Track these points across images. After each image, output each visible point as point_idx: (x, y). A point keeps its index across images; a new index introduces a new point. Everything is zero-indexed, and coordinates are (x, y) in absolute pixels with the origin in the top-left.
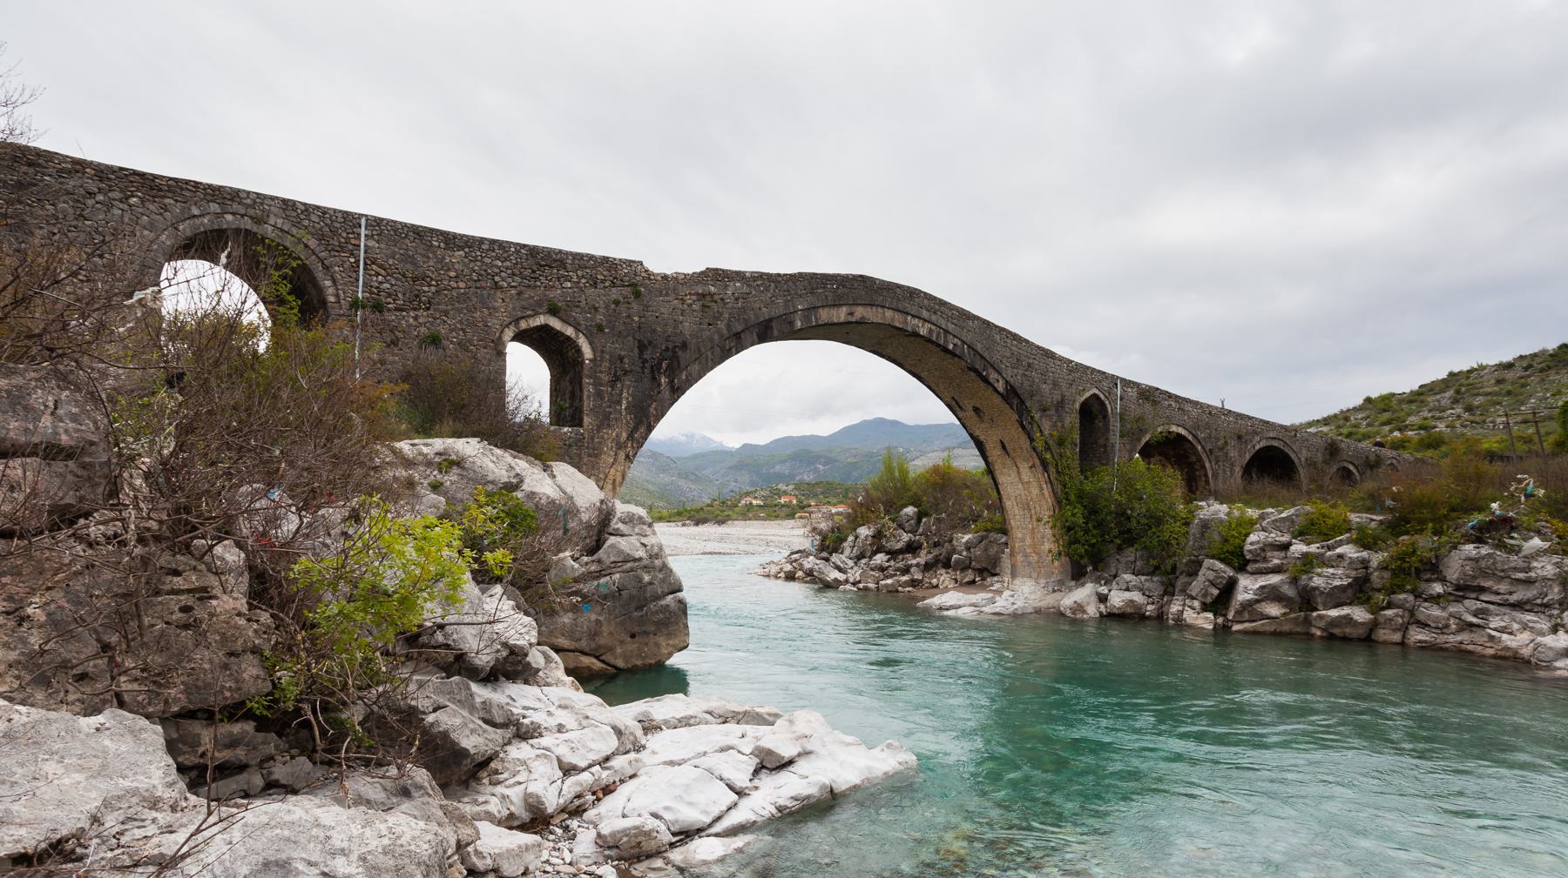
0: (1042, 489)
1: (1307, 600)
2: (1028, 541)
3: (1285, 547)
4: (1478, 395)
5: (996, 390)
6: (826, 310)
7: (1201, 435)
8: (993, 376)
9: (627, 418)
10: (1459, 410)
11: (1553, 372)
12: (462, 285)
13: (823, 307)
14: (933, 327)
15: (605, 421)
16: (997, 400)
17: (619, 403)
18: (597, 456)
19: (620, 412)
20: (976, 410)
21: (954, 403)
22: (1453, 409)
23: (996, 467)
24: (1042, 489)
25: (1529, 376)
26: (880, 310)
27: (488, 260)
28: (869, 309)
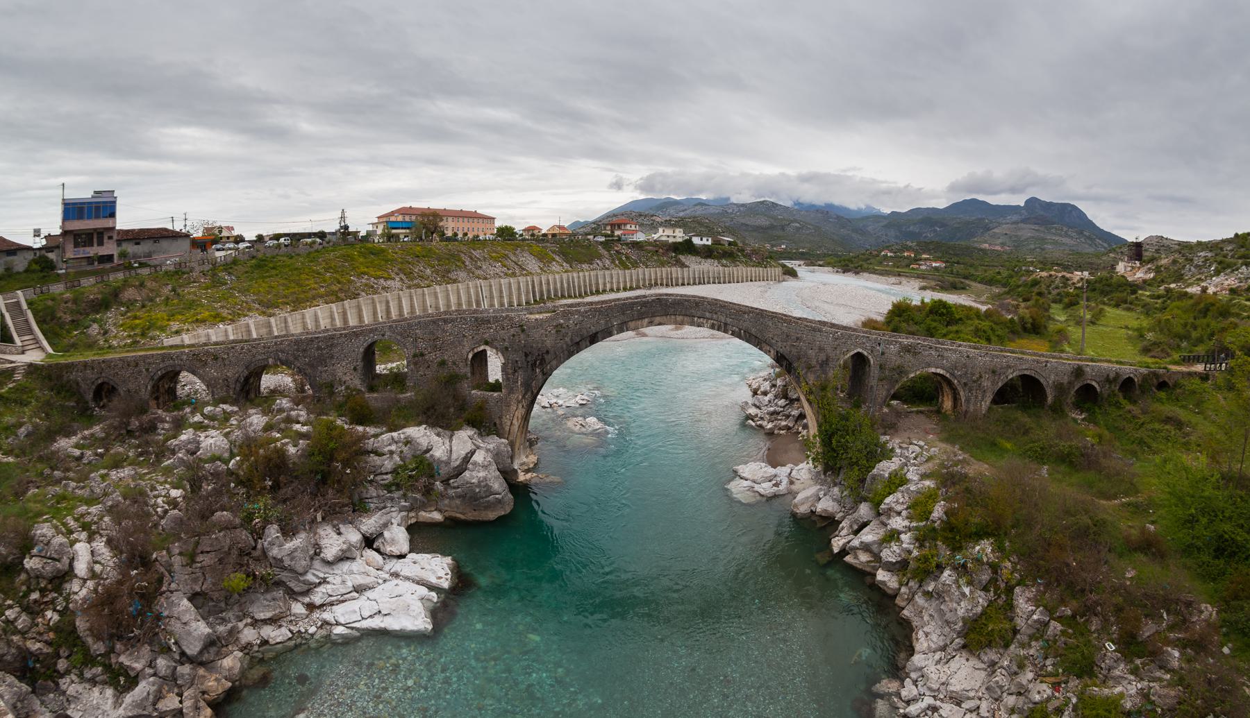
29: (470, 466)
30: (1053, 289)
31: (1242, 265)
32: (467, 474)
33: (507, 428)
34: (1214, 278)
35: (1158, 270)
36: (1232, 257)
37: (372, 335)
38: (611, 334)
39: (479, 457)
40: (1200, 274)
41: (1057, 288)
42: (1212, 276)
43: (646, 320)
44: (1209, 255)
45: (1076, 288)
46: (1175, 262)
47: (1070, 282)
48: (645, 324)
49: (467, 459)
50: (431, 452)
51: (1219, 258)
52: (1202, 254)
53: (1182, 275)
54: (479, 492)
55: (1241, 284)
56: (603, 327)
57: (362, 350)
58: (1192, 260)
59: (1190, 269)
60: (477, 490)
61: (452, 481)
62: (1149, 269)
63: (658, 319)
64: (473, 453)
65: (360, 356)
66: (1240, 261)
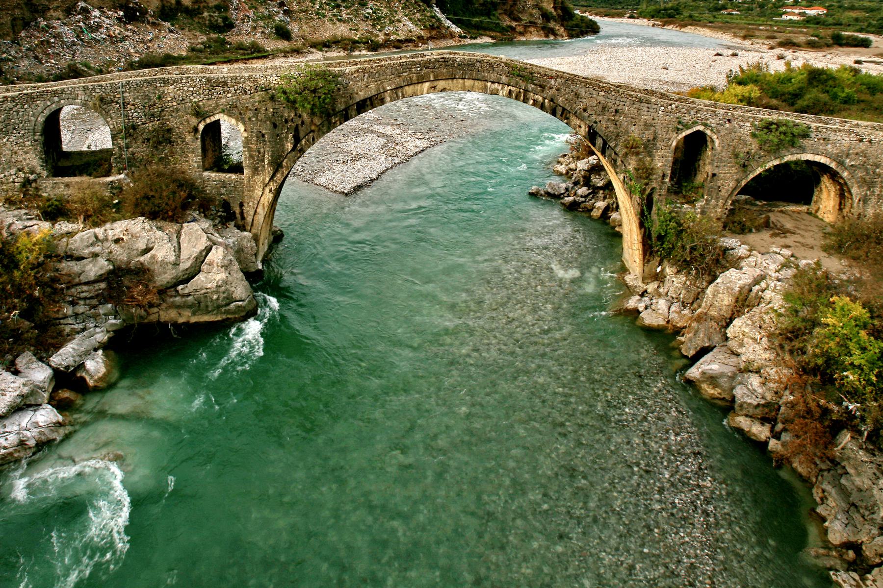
6: (411, 87)
9: (269, 170)
12: (175, 104)
13: (408, 85)
14: (513, 89)
15: (255, 171)
17: (263, 161)
18: (253, 191)
19: (264, 167)
26: (460, 81)
27: (186, 88)
28: (450, 81)
29: (204, 267)
32: (201, 277)
33: (249, 219)
37: (56, 99)
38: (382, 102)
39: (217, 255)
43: (427, 85)
48: (425, 90)
49: (200, 260)
50: (152, 252)
54: (218, 299)
56: (374, 93)
57: (41, 119)
60: (215, 297)
61: (180, 287)
63: (441, 84)
64: (208, 250)
65: (39, 128)
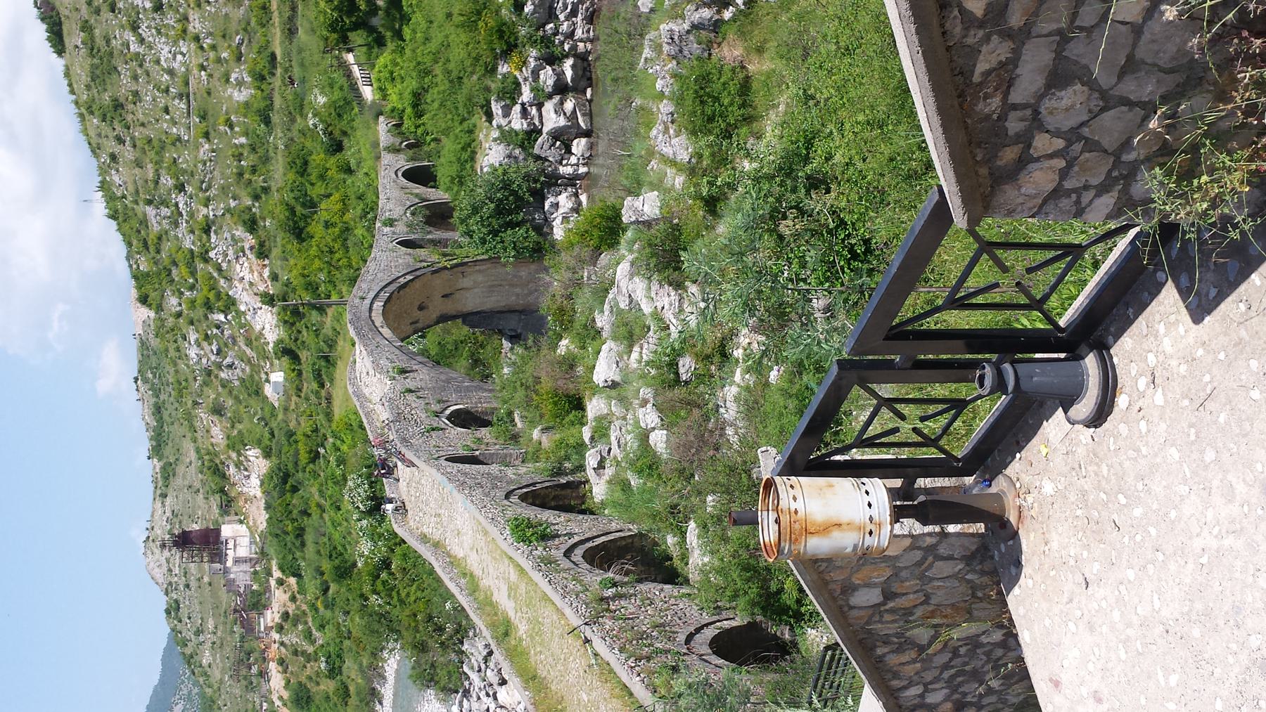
0: (479, 271)
1: (561, 89)
2: (518, 290)
3: (523, 104)
4: (157, 183)
5: (413, 280)
7: (409, 203)
8: (402, 280)
10: (181, 200)
11: (129, 117)
16: (417, 284)
20: (421, 308)
21: (414, 326)
22: (177, 205)
23: (460, 309)
24: (479, 271)
25: (133, 138)
30: (313, 642)
31: (206, 260)
34: (243, 308)
35: (237, 444)
36: (192, 288)
40: (235, 342)
41: (308, 636)
42: (240, 314)
44: (193, 337)
45: (302, 590)
46: (218, 411)
47: (291, 608)
51: (200, 312)
52: (193, 352)
53: (242, 381)
55: (247, 246)
58: (209, 373)
59: (230, 366)
62: (238, 465)
66: (200, 266)
